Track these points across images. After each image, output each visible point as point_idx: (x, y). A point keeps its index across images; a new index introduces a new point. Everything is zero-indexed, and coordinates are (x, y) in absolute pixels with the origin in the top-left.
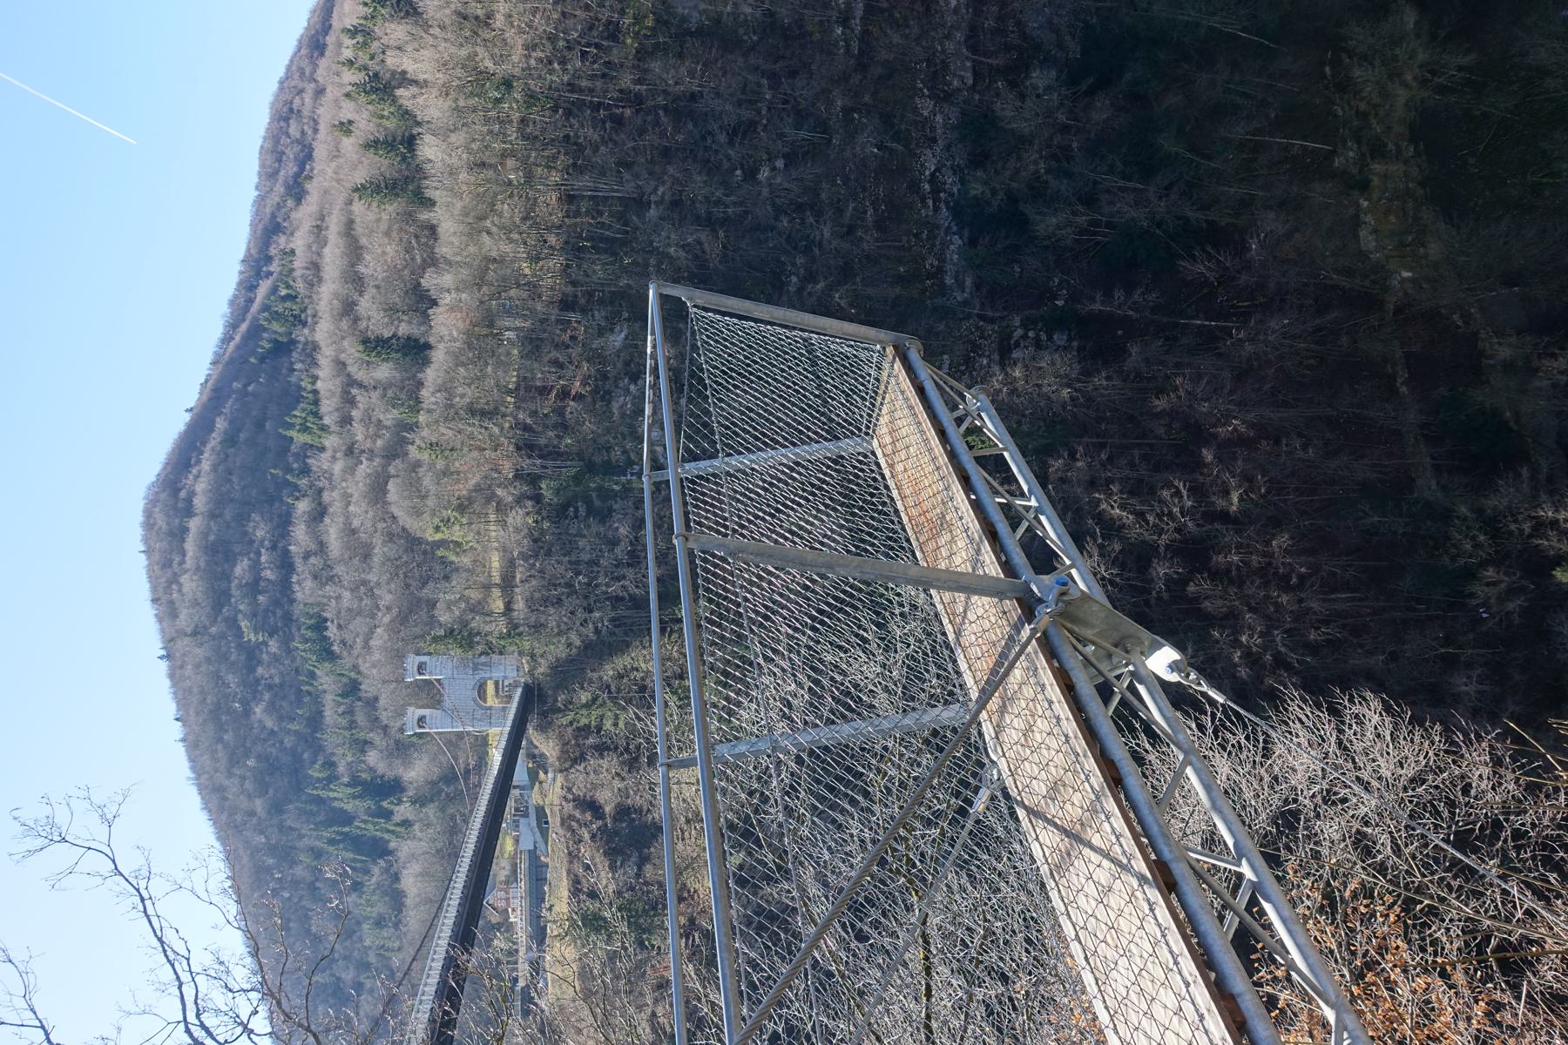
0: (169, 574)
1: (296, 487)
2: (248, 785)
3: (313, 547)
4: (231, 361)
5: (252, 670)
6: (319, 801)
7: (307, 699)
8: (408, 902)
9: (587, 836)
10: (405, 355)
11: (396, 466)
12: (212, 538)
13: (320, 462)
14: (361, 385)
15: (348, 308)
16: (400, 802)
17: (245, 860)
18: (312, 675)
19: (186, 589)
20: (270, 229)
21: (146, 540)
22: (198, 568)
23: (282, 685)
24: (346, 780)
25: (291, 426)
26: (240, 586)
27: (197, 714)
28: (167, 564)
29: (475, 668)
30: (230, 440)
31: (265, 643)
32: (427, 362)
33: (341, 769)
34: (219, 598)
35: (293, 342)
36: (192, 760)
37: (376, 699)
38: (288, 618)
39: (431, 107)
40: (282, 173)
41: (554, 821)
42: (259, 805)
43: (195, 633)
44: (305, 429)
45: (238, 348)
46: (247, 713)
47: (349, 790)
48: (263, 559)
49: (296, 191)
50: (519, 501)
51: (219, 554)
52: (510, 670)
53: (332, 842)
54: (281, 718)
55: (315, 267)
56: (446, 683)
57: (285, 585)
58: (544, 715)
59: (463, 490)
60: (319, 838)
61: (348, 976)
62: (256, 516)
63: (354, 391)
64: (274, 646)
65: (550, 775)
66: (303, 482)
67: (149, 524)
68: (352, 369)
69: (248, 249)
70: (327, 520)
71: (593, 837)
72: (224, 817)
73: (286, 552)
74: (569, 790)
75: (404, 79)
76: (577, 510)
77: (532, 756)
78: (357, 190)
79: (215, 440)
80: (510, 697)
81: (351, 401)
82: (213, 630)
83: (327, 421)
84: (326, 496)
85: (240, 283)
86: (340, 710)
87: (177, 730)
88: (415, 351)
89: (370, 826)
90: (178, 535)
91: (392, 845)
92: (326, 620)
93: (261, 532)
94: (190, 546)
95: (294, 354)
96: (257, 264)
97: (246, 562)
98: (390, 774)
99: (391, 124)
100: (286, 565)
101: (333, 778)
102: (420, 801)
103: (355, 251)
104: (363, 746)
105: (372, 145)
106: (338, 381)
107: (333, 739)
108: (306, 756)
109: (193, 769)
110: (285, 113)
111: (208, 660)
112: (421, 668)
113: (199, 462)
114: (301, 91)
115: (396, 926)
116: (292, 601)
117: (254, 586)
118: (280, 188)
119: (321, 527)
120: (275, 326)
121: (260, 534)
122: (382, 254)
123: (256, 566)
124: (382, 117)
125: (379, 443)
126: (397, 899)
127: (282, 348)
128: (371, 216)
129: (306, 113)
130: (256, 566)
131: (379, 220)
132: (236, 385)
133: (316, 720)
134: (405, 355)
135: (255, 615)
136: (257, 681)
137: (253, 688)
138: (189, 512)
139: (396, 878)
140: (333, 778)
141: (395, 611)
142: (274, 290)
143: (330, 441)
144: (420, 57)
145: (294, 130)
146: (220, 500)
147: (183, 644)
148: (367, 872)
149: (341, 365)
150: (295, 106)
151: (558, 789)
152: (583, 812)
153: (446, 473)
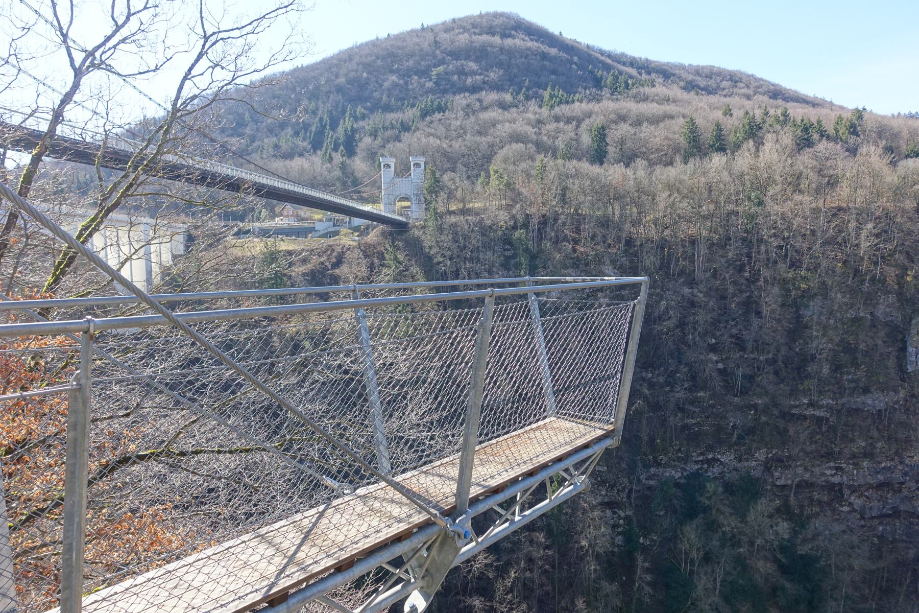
0: (469, 27)
1: (518, 93)
2: (352, 74)
3: (485, 104)
4: (590, 56)
5: (416, 74)
6: (344, 112)
7: (400, 103)
8: (288, 162)
9: (322, 259)
10: (596, 150)
11: (532, 148)
12: (489, 49)
13: (533, 105)
14: (578, 126)
15: (622, 118)
16: (343, 156)
17: (312, 74)
18: (413, 106)
19: (461, 36)
20: (666, 73)
21: (488, 14)
22: (472, 42)
23: (408, 90)
24: (355, 126)
25: (553, 89)
26: (462, 65)
27: (392, 45)
28: (474, 26)
29: (417, 195)
30: (544, 56)
31: (431, 80)
32: (592, 162)
33: (361, 123)
34: (455, 54)
35: (601, 89)
36: (367, 44)
37: (400, 141)
38: (445, 92)
39: (743, 160)
40: (699, 78)
41: (331, 241)
42: (342, 80)
43: (436, 42)
44: (552, 96)
45: (597, 59)
46: (392, 72)
47: (349, 128)
48: (478, 77)
49: (690, 86)
50: (513, 216)
51: (481, 54)
52: (416, 214)
53: (321, 119)
54: (389, 90)
55: (645, 99)
56: (409, 179)
57: (463, 89)
58: (391, 234)
59: (519, 185)
60: (323, 112)
61: (248, 131)
62: (501, 72)
63: (574, 123)
64: (429, 84)
65: (357, 238)
66: (521, 97)
67: (496, 15)
68: (587, 121)
69: (654, 62)
70: (500, 111)
71: (322, 263)
72: (336, 62)
73: (481, 89)
74: (348, 249)
75: (759, 144)
76: (508, 250)
77: (367, 228)
78: (692, 120)
79: (545, 48)
80: (401, 215)
81: (568, 121)
82: (438, 52)
83: (557, 109)
84: (514, 110)
85: (634, 58)
86: (394, 122)
87: (383, 35)
88: (599, 157)
89: (329, 140)
90: (491, 31)
91: (319, 152)
92: (444, 112)
93: (493, 75)
94: (485, 38)
95: (594, 90)
96: (646, 67)
97: (476, 68)
98: (358, 150)
99: (731, 138)
100: (474, 89)
101: (356, 119)
102: (343, 167)
103: (655, 121)
104: (374, 134)
105: (719, 128)
106: (579, 114)
107: (377, 119)
108: (368, 104)
109: (362, 45)
110: (734, 79)
111: (421, 50)
112: (417, 165)
113: (532, 40)
114: (748, 87)
115: (275, 156)
116: (454, 93)
117: (462, 73)
118: (690, 77)
119: (496, 108)
120: (610, 78)
121: (492, 75)
122: (655, 136)
123: (473, 73)
124: (736, 133)
125: (545, 138)
126: (289, 156)
127: (598, 83)
128: (676, 129)
129: (735, 90)
130: (473, 73)
131: (674, 133)
132: (576, 59)
133: (388, 108)
134: (596, 150)
135: (446, 74)
136: (410, 76)
137: (406, 74)
138: (504, 36)
139: (301, 155)
140: (356, 119)
141: (449, 150)
142: (631, 77)
143: (545, 112)
144: (772, 153)
145: (725, 84)
146: (510, 52)
147: (430, 37)
148: (304, 139)
149: (589, 115)
150: (739, 84)
151: (349, 242)
152: (336, 257)
153: (529, 176)
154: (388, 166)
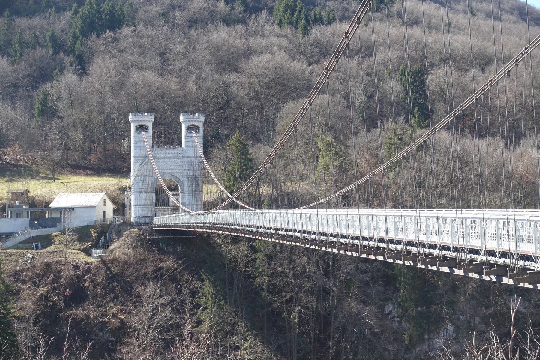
9: (43, 290)
18: (59, 10)
41: (45, 255)
55: (415, 22)
56: (178, 150)
71: (43, 298)
74: (88, 271)
84: (240, 27)
154: (141, 128)
